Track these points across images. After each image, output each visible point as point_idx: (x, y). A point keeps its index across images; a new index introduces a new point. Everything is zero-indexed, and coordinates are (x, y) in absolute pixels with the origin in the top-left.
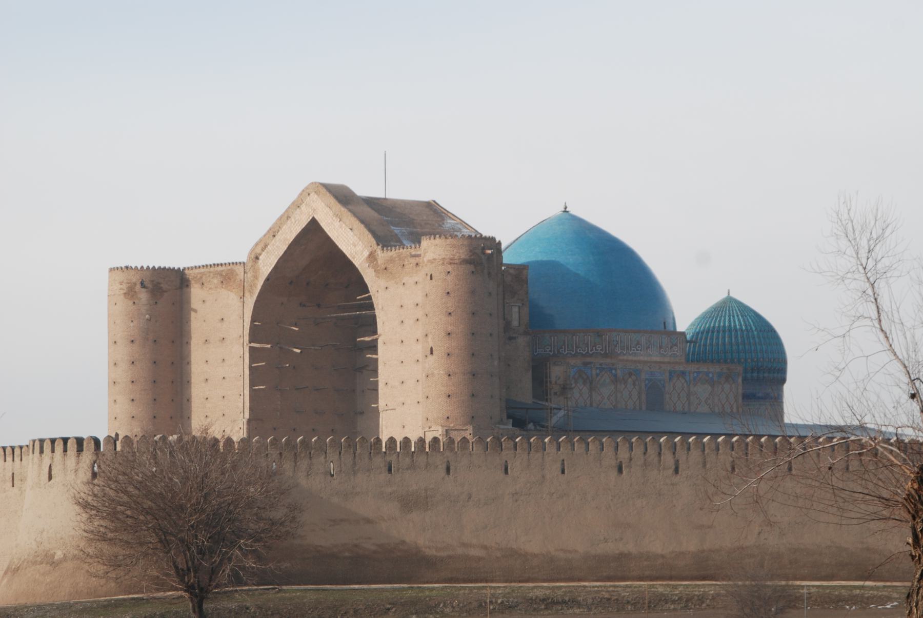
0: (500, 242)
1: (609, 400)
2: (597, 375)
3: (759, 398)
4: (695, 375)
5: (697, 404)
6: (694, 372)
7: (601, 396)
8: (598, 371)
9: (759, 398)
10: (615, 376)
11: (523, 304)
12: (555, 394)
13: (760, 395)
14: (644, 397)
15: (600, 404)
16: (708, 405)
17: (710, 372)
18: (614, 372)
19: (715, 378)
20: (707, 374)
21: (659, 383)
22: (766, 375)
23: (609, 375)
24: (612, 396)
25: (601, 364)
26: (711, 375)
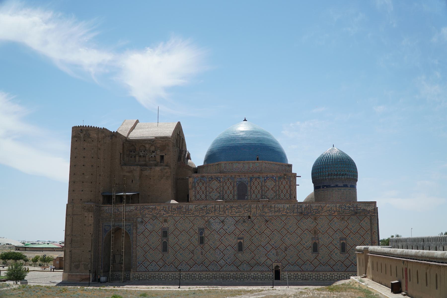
0: (103, 128)
1: (216, 190)
2: (210, 181)
3: (332, 187)
4: (265, 178)
5: (267, 190)
6: (265, 177)
7: (212, 189)
8: (210, 179)
9: (332, 187)
10: (220, 180)
11: (165, 154)
12: (190, 189)
13: (333, 185)
14: (235, 188)
15: (211, 192)
16: (273, 191)
17: (274, 177)
18: (219, 179)
19: (277, 179)
20: (273, 177)
21: (244, 182)
22: (341, 177)
23: (216, 181)
24: (218, 189)
25: (211, 176)
26: (274, 178)
